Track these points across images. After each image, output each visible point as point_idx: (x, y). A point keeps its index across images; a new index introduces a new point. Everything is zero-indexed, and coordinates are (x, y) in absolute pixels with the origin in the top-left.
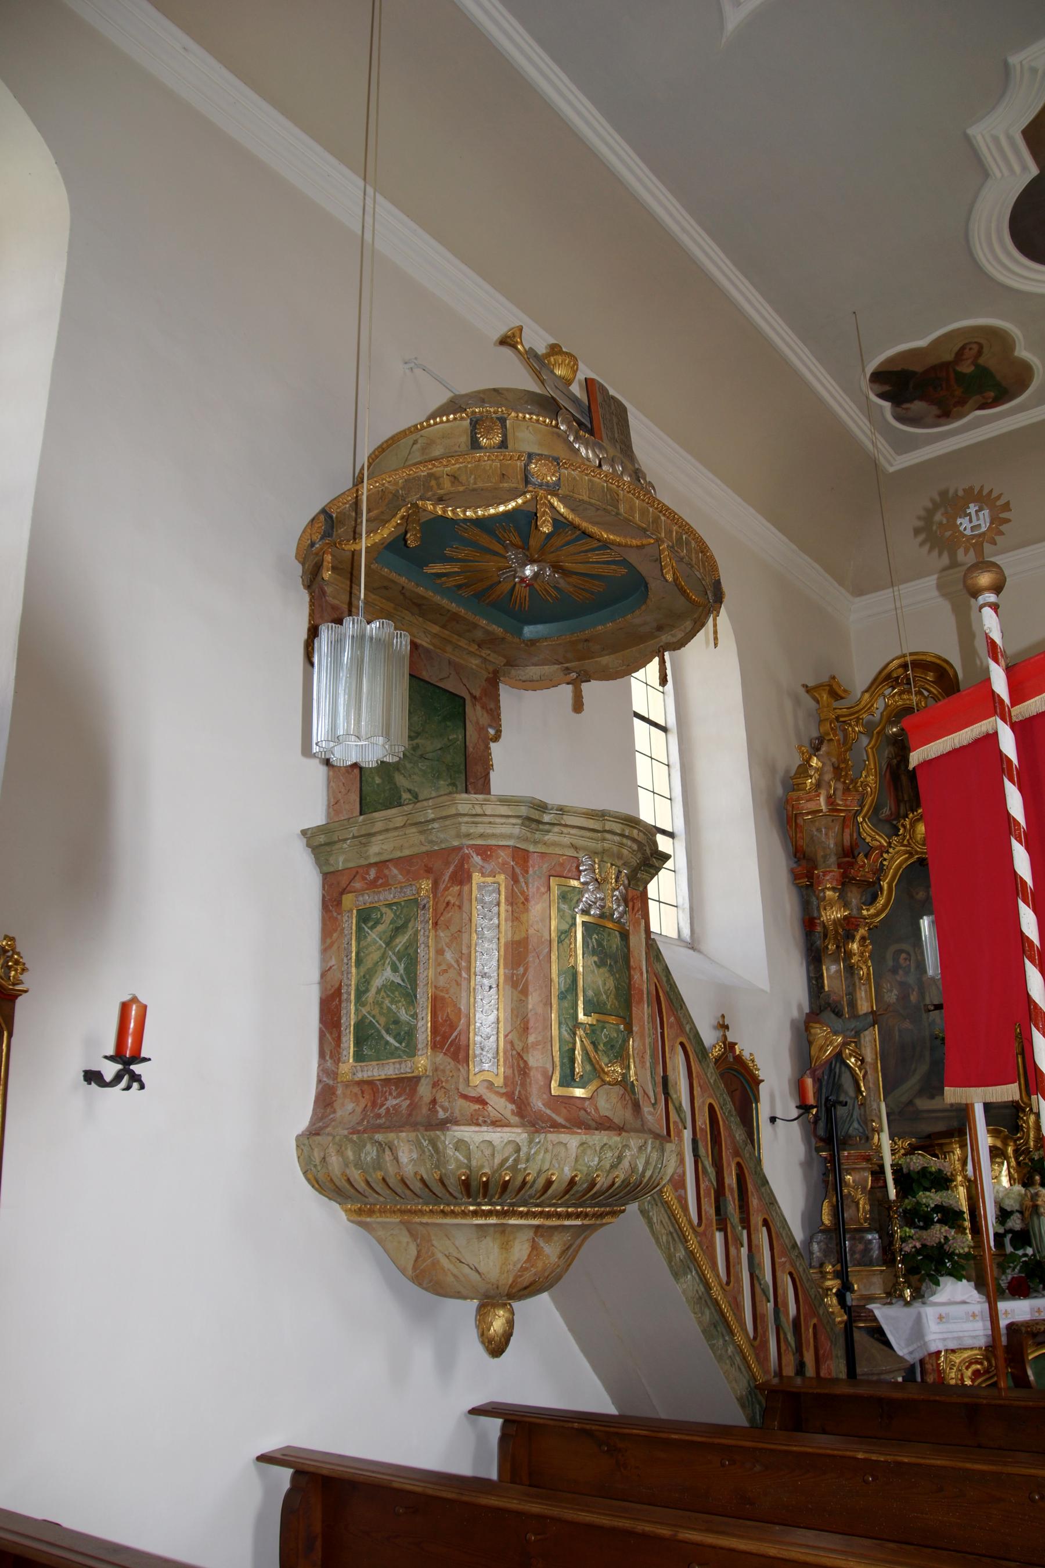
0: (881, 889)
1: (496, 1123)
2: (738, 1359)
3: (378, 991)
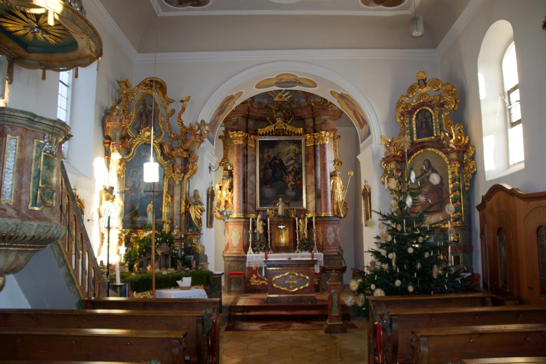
0: (131, 150)
1: (10, 217)
2: (76, 293)
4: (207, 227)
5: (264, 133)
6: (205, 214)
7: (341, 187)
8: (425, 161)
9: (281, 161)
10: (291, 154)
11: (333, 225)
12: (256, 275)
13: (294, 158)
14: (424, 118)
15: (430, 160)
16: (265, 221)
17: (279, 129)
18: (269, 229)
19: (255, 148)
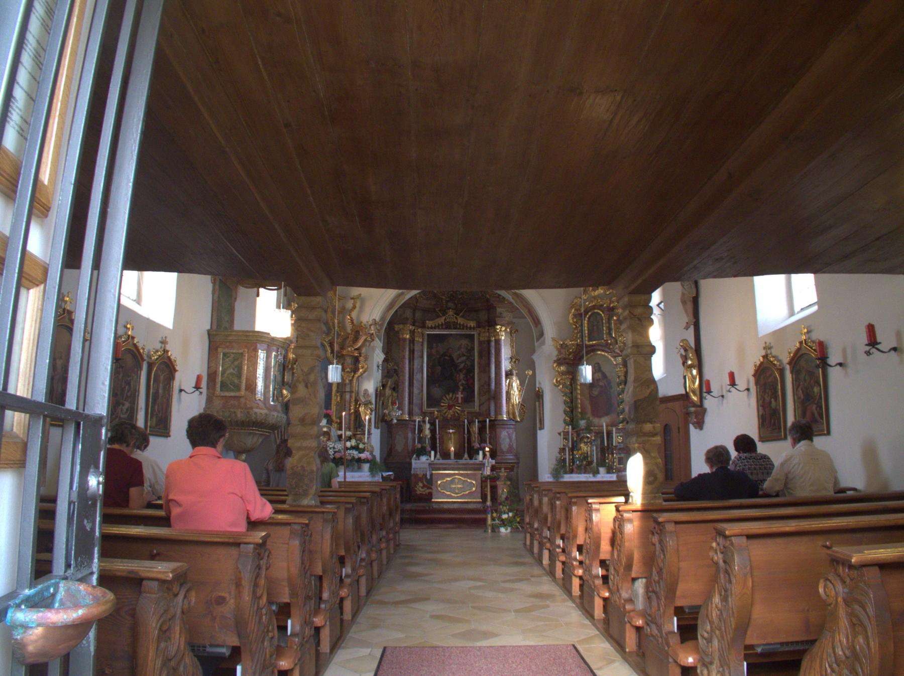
3: (228, 374)
4: (375, 427)
5: (433, 326)
6: (374, 413)
7: (518, 388)
8: (596, 363)
9: (450, 356)
10: (463, 350)
11: (507, 430)
12: (422, 482)
13: (466, 354)
15: (600, 362)
16: (433, 424)
17: (449, 322)
18: (438, 433)
19: (423, 342)
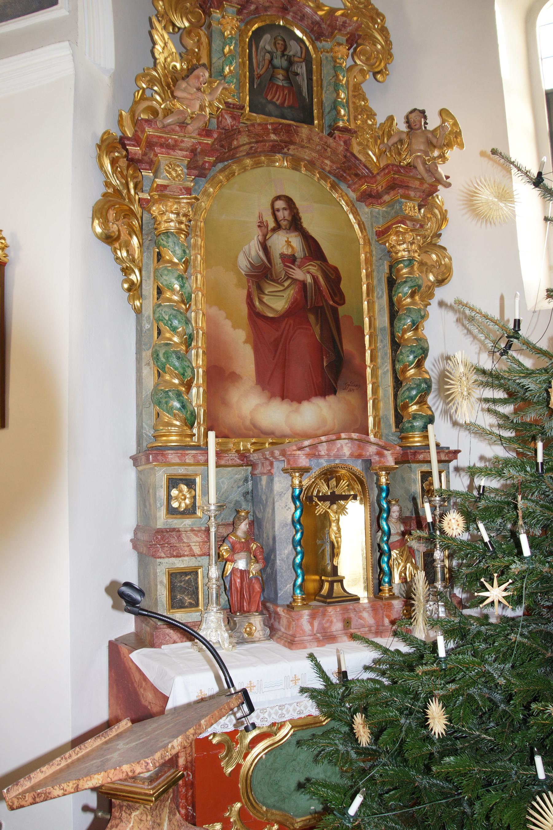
8: (278, 198)
14: (283, 55)
